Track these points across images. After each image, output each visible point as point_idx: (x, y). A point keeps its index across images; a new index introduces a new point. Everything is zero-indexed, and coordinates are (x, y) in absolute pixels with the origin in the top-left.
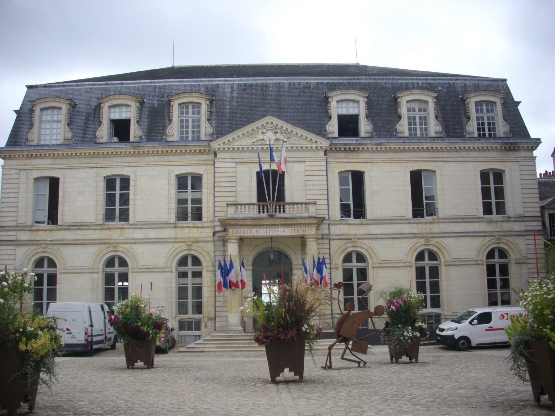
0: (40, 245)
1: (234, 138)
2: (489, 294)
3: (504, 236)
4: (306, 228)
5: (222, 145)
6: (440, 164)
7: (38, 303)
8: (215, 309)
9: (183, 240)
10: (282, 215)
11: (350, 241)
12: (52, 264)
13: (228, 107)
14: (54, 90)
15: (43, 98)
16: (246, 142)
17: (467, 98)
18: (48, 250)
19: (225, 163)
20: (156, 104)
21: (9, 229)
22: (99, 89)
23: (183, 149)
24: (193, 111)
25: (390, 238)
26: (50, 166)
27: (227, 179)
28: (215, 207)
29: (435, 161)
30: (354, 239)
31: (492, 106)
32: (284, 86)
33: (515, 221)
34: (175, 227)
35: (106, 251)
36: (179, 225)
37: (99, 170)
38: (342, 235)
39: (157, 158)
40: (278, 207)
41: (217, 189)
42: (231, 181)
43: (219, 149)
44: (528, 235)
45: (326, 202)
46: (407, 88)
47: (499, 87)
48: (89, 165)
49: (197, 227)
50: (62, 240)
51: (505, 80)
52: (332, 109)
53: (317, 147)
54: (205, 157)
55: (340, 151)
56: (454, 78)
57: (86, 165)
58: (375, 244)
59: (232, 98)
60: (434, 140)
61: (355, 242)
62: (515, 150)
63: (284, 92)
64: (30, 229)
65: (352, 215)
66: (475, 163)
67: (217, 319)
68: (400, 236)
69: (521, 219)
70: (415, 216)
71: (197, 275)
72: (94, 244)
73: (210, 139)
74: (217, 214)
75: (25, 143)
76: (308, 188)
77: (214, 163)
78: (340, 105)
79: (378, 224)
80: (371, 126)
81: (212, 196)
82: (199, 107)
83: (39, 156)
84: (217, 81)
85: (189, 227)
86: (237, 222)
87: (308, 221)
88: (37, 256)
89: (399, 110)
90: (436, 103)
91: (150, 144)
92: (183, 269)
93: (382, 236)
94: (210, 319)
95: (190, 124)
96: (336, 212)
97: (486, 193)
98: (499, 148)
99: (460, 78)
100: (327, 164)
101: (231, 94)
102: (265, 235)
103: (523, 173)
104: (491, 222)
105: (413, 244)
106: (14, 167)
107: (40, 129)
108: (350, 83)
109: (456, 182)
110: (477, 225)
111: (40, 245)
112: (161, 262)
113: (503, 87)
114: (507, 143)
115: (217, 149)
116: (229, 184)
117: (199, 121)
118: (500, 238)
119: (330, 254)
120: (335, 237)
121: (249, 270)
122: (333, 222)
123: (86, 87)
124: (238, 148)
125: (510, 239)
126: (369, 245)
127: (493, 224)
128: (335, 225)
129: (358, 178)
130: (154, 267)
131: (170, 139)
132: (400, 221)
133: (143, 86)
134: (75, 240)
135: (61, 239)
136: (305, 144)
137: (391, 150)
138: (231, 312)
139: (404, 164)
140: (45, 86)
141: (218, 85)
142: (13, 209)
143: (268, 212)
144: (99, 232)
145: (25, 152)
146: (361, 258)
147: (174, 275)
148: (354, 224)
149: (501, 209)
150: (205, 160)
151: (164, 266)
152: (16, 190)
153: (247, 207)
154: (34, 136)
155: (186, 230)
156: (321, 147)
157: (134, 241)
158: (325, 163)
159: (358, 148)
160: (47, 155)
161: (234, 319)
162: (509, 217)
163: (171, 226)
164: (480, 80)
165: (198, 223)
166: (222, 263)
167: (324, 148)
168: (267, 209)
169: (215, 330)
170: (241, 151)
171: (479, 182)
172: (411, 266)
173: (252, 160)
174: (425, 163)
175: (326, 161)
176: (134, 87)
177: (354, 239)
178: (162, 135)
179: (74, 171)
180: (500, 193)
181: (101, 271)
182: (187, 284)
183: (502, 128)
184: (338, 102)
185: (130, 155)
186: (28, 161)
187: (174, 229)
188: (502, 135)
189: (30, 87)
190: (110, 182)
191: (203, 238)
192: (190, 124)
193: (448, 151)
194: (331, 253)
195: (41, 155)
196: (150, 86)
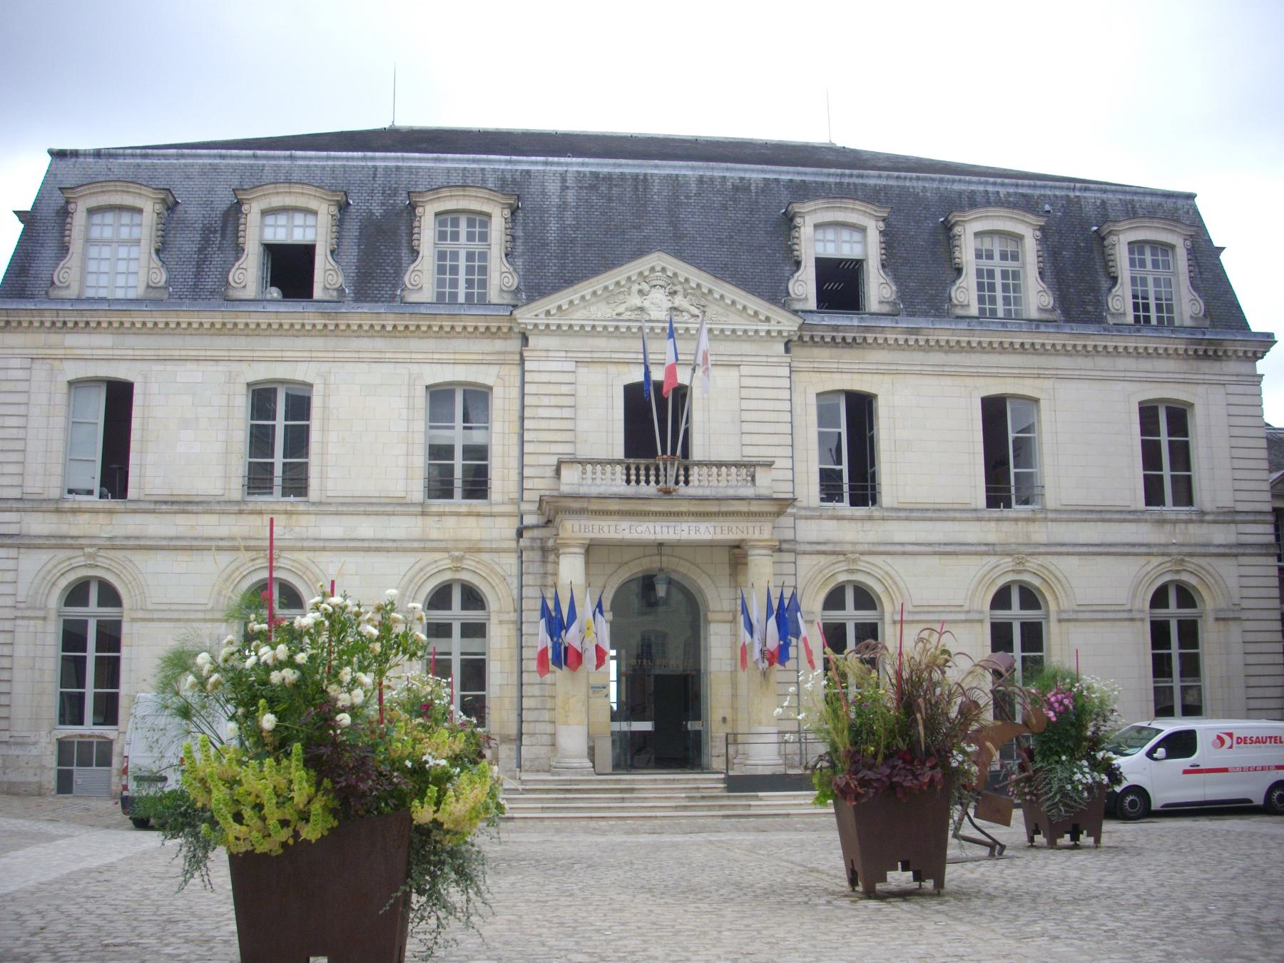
0: (81, 548)
1: (571, 302)
2: (1155, 688)
3: (1191, 555)
5: (543, 316)
6: (1048, 384)
7: (70, 695)
8: (520, 715)
9: (443, 545)
11: (841, 558)
12: (110, 596)
13: (553, 226)
14: (120, 165)
15: (91, 183)
16: (601, 312)
17: (1110, 232)
18: (100, 561)
19: (549, 363)
20: (378, 211)
22: (234, 169)
23: (447, 324)
25: (935, 553)
26: (110, 352)
27: (554, 401)
29: (1039, 376)
30: (852, 553)
31: (1165, 253)
32: (687, 183)
33: (1215, 522)
34: (423, 514)
36: (434, 509)
37: (235, 367)
38: (825, 543)
39: (380, 343)
42: (563, 404)
43: (536, 326)
44: (1244, 555)
46: (972, 202)
47: (1178, 210)
48: (209, 353)
49: (478, 515)
50: (137, 538)
51: (1191, 197)
52: (803, 244)
53: (768, 332)
54: (499, 345)
55: (823, 343)
56: (1078, 185)
57: (203, 353)
58: (898, 566)
59: (563, 206)
60: (1038, 327)
61: (854, 561)
62: (1216, 357)
63: (688, 197)
65: (846, 496)
66: (1126, 384)
68: (957, 549)
69: (1229, 516)
70: (992, 502)
71: (475, 631)
75: (47, 293)
76: (746, 428)
77: (522, 361)
78: (820, 235)
79: (907, 519)
80: (894, 288)
82: (485, 224)
83: (82, 325)
86: (585, 505)
88: (72, 577)
89: (957, 254)
91: (366, 308)
92: (440, 615)
93: (916, 549)
94: (505, 739)
95: (462, 263)
96: (810, 491)
97: (1151, 456)
98: (1181, 352)
99: (1092, 186)
102: (652, 537)
103: (1233, 410)
104: (1162, 522)
105: (987, 568)
106: (16, 351)
107: (85, 258)
108: (841, 184)
109: (1086, 427)
110: (1131, 527)
111: (81, 548)
113: (1188, 212)
114: (1200, 342)
115: (530, 327)
116: (557, 413)
117: (483, 256)
118: (1183, 560)
120: (808, 548)
122: (803, 513)
123: (201, 161)
124: (582, 327)
125: (1203, 562)
126: (887, 568)
127: (1168, 527)
128: (807, 518)
129: (861, 409)
131: (413, 298)
132: (958, 515)
133: (344, 166)
134: (171, 539)
135: (137, 533)
136: (741, 324)
137: (939, 347)
138: (566, 723)
139: (969, 381)
140: (98, 154)
141: (528, 172)
143: (657, 482)
145: (47, 313)
146: (865, 599)
148: (852, 519)
149: (1185, 493)
150: (499, 353)
152: (22, 410)
153: (608, 468)
154: (69, 275)
155: (451, 522)
156: (780, 332)
157: (321, 544)
159: (865, 339)
160: (104, 325)
161: (573, 740)
162: (1203, 513)
163: (412, 509)
164: (1136, 193)
165: (478, 505)
166: (551, 605)
167: (785, 334)
168: (657, 476)
169: (520, 766)
170: (588, 335)
172: (981, 621)
173: (614, 355)
174: (1017, 380)
176: (324, 168)
177: (852, 553)
178: (395, 287)
179: (170, 367)
180: (1182, 455)
182: (450, 654)
183: (1187, 306)
184: (817, 226)
185: (313, 332)
186: (54, 338)
187: (420, 519)
188: (1188, 322)
189: (58, 155)
190: (261, 399)
192: (462, 263)
193: (1067, 354)
195: (87, 323)
196: (363, 167)
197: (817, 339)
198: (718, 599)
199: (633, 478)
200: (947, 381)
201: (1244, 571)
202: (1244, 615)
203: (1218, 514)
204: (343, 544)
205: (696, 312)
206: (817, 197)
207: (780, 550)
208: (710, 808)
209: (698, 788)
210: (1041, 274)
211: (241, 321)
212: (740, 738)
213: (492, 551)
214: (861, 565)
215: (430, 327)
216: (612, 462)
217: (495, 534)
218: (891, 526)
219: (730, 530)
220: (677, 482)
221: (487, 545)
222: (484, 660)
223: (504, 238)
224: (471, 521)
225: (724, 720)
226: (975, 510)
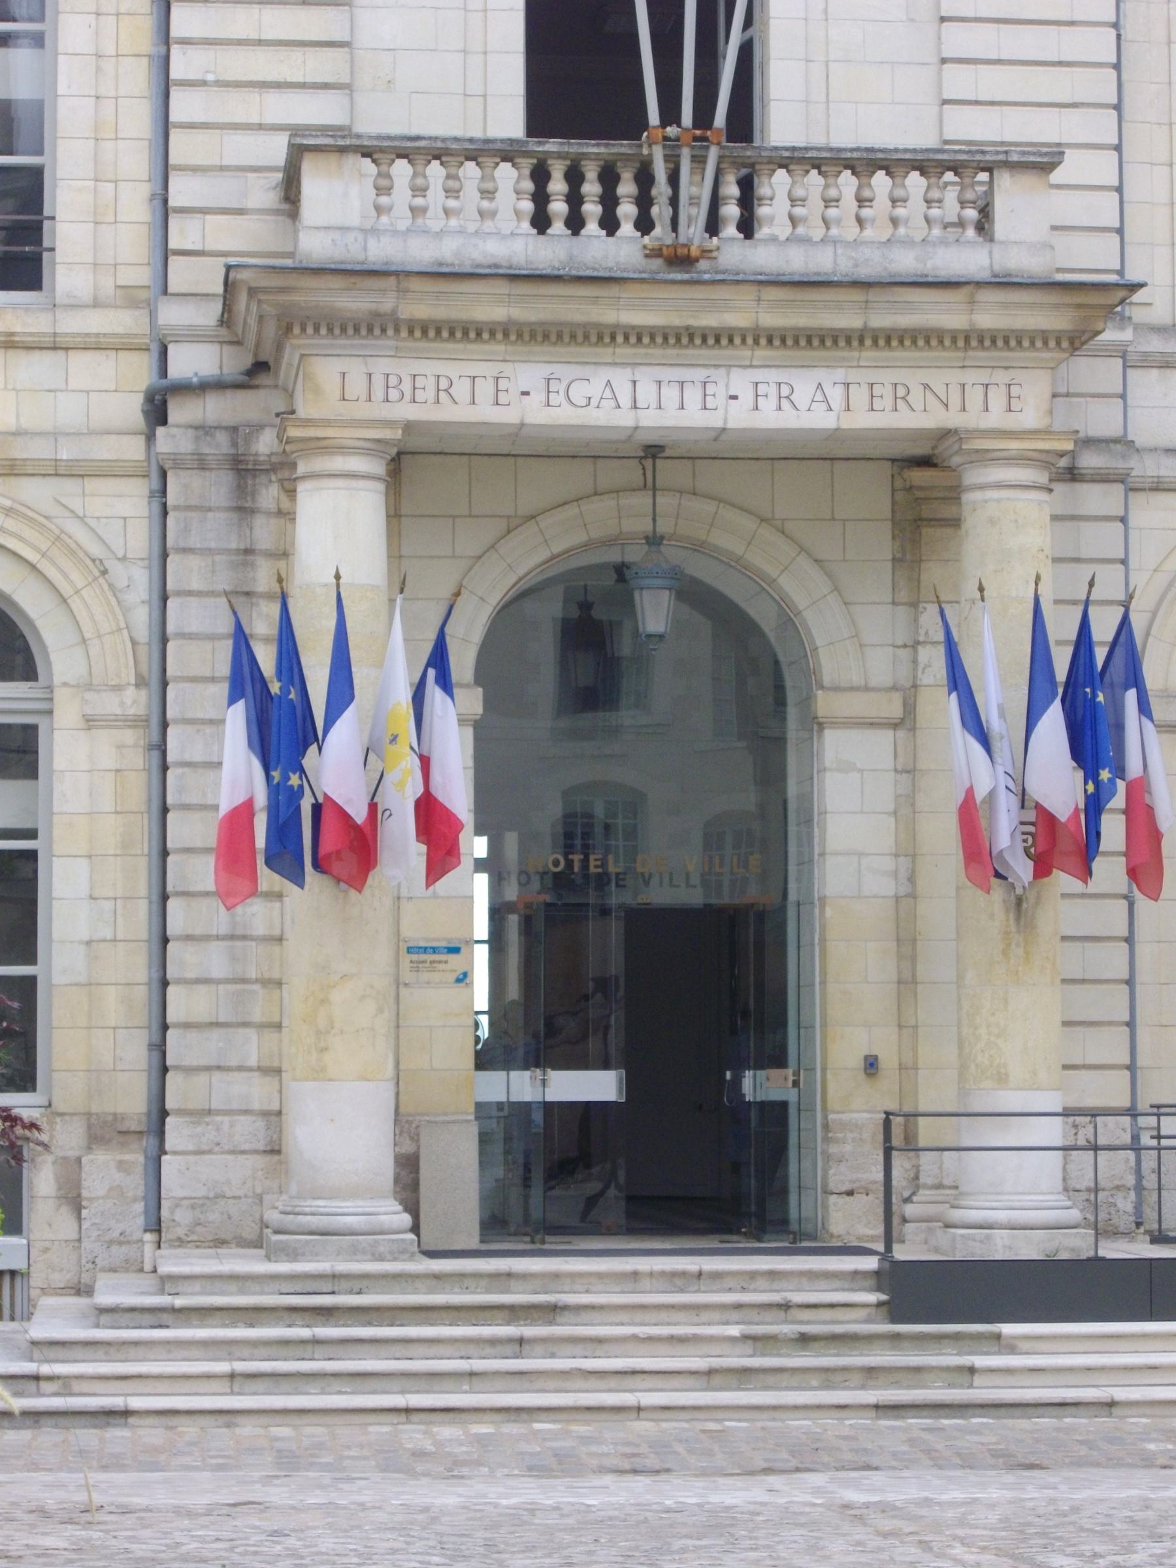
4: (972, 377)
8: (160, 1048)
67: (176, 1132)
86: (387, 303)
94: (103, 1131)
102: (625, 419)
122: (1155, 344)
138: (319, 1074)
143: (644, 224)
161: (343, 1135)
168: (644, 201)
169: (156, 1226)
191: (55, 435)
198: (850, 641)
199: (558, 207)
207: (1072, 475)
208: (829, 1377)
209: (786, 1306)
212: (927, 1132)
213: (58, 471)
216: (483, 152)
217: (68, 411)
219: (900, 397)
220: (713, 226)
221: (38, 450)
222: (32, 855)
225: (871, 1065)
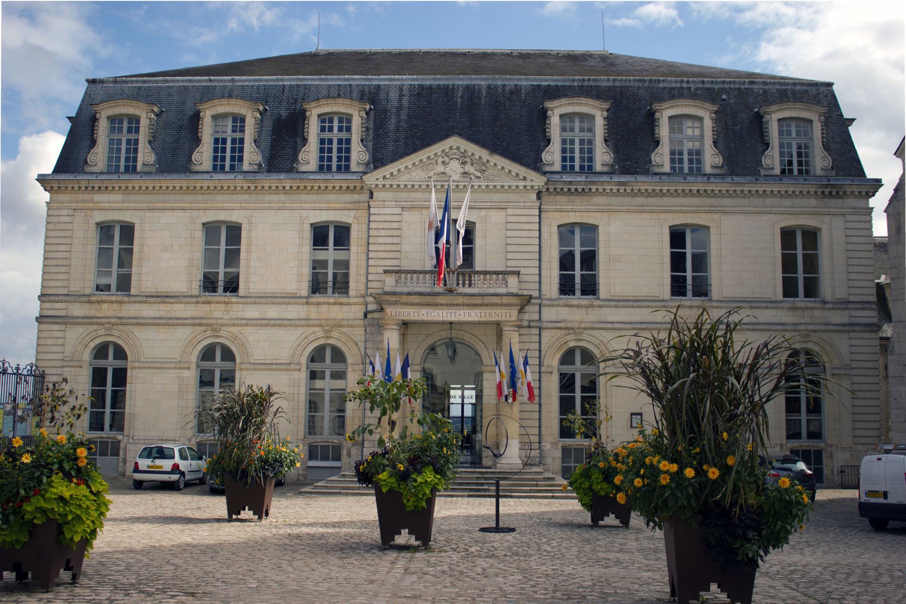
1: (399, 170)
2: (787, 420)
3: (815, 331)
5: (381, 179)
6: (716, 216)
10: (467, 290)
11: (571, 331)
12: (120, 354)
14: (129, 87)
15: (110, 98)
16: (418, 175)
18: (114, 332)
19: (385, 209)
20: (284, 114)
21: (57, 298)
22: (198, 88)
24: (339, 127)
27: (388, 233)
28: (368, 274)
29: (710, 212)
32: (480, 90)
33: (833, 309)
34: (307, 303)
35: (203, 336)
37: (195, 213)
40: (461, 278)
41: (371, 247)
43: (377, 185)
44: (854, 331)
45: (537, 271)
48: (179, 205)
49: (341, 304)
50: (136, 318)
51: (830, 85)
53: (525, 187)
54: (356, 197)
57: (176, 205)
59: (400, 108)
60: (708, 179)
61: (580, 334)
62: (838, 196)
64: (86, 299)
66: (772, 216)
69: (844, 304)
72: (184, 325)
73: (365, 170)
74: (371, 285)
76: (510, 248)
79: (616, 306)
81: (364, 257)
83: (103, 188)
84: (375, 80)
85: (328, 304)
87: (505, 300)
88: (98, 341)
89: (657, 131)
90: (716, 121)
91: (274, 176)
92: (317, 366)
93: (622, 326)
97: (788, 264)
98: (812, 193)
100: (540, 212)
101: (400, 101)
102: (441, 319)
104: (794, 309)
106: (65, 205)
108: (582, 86)
109: (743, 246)
110: (772, 312)
112: (284, 355)
113: (826, 96)
114: (826, 186)
116: (389, 240)
117: (348, 141)
119: (540, 351)
120: (549, 325)
121: (416, 371)
122: (547, 302)
125: (825, 336)
126: (602, 338)
128: (549, 306)
130: (274, 362)
131: (303, 168)
133: (265, 85)
134: (156, 318)
135: (136, 315)
137: (640, 193)
139: (661, 216)
140: (115, 80)
141: (379, 86)
142: (63, 269)
143: (445, 285)
144: (193, 307)
145: (82, 182)
147: (303, 375)
149: (812, 289)
150: (355, 202)
151: (288, 362)
152: (68, 241)
155: (324, 308)
156: (532, 187)
157: (245, 322)
158: (537, 212)
160: (117, 188)
162: (824, 302)
170: (409, 191)
171: (778, 245)
174: (694, 215)
175: (540, 208)
176: (252, 86)
179: (156, 214)
180: (812, 263)
181: (194, 366)
183: (820, 161)
186: (87, 196)
189: (92, 82)
192: (335, 146)
193: (730, 196)
194: (542, 349)
195: (107, 188)
196: (276, 86)
197: (559, 190)
200: (647, 216)
201: (853, 342)
202: (853, 372)
203: (836, 303)
204: (259, 322)
205: (479, 174)
206: (565, 96)
210: (715, 143)
211: (198, 185)
213: (349, 326)
214: (584, 336)
215: (312, 187)
217: (351, 316)
218: (605, 311)
220: (458, 284)
221: (346, 322)
223: (360, 129)
224: (337, 307)
226: (663, 301)
